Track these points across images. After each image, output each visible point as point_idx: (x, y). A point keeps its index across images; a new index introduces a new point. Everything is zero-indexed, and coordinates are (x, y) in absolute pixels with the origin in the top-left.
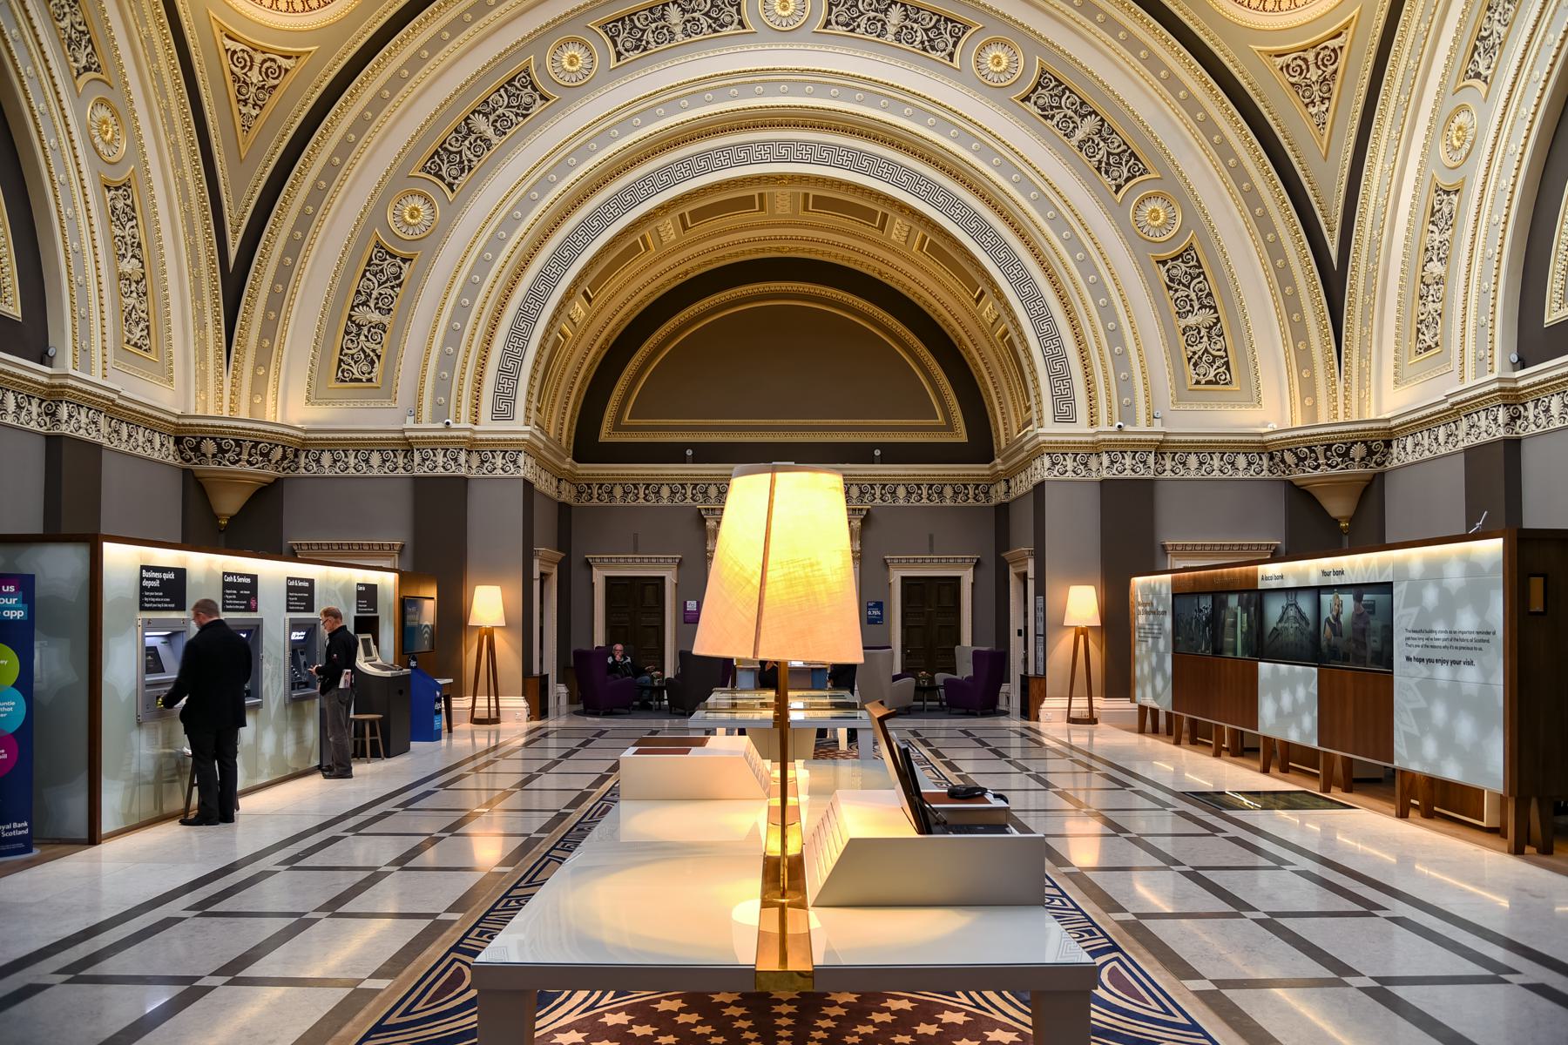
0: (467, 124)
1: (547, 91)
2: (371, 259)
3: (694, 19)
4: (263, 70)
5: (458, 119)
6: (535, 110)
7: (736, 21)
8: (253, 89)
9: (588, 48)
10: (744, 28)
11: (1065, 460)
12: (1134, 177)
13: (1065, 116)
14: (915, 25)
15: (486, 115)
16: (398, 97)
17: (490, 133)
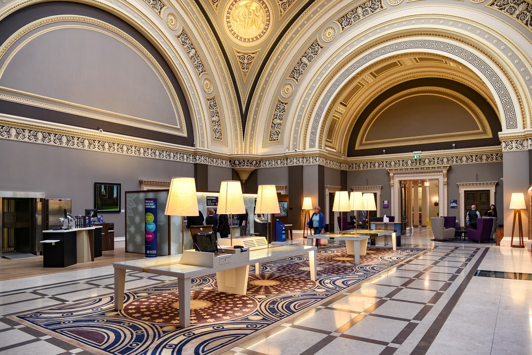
0: (301, 61)
2: (277, 105)
4: (248, 59)
5: (298, 60)
7: (380, 6)
8: (245, 65)
10: (382, 8)
11: (512, 143)
15: (306, 57)
16: (282, 57)
17: (307, 62)
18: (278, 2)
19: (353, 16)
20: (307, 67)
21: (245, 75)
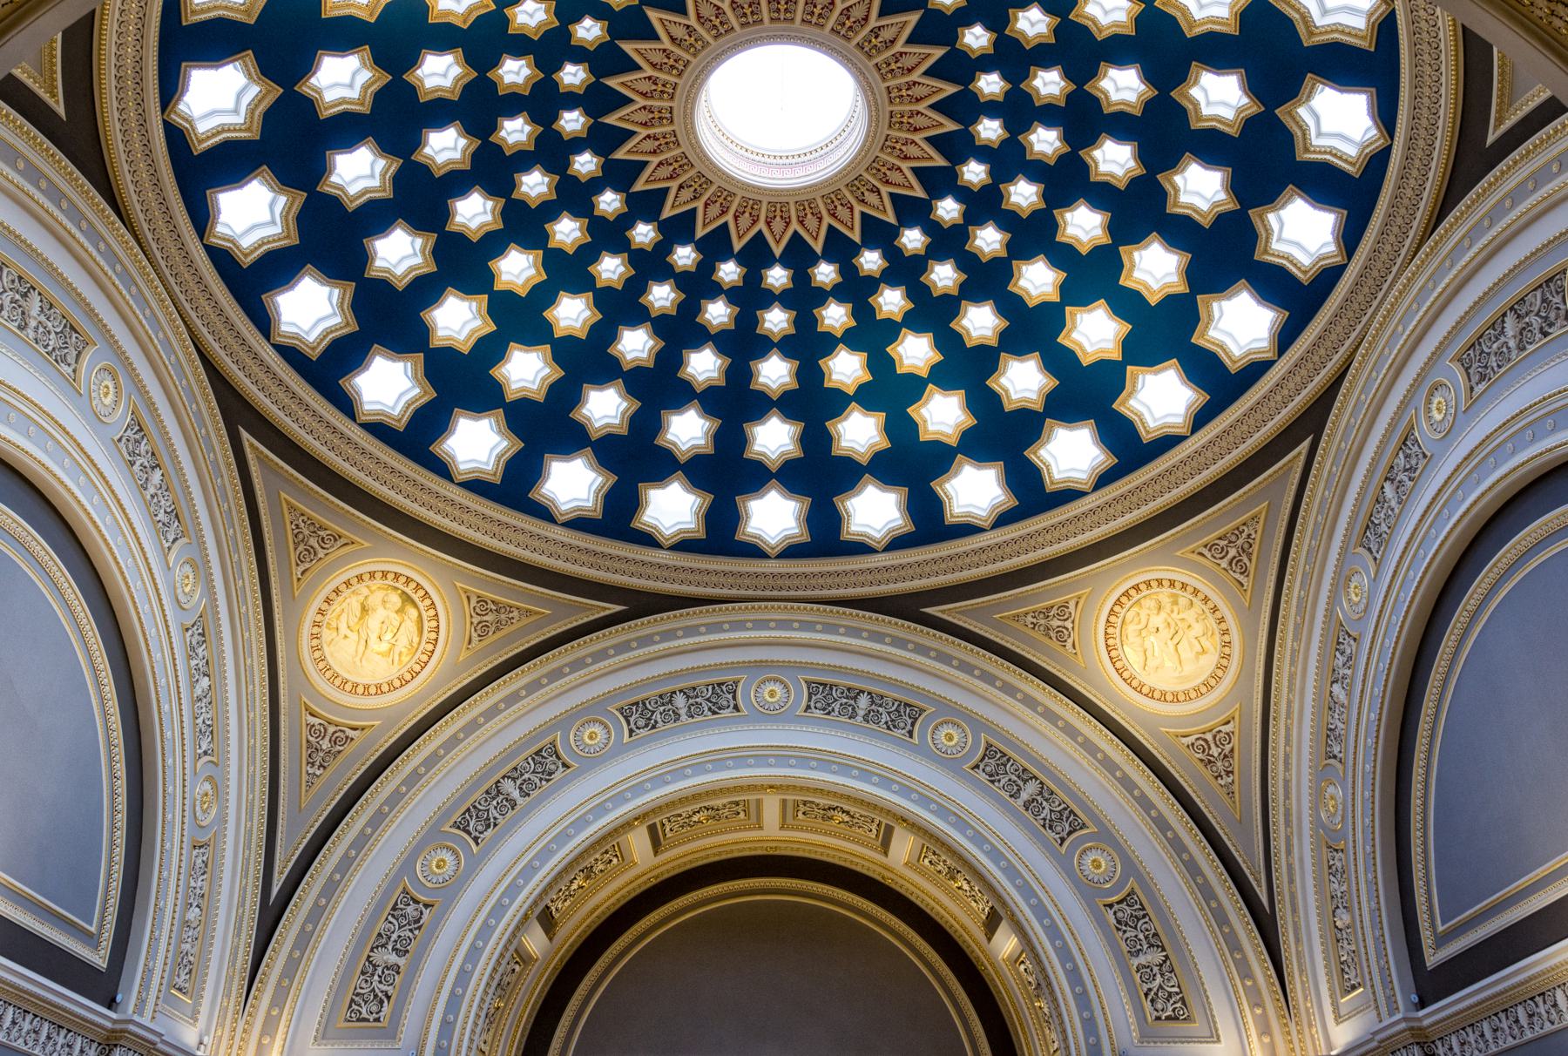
0: (497, 787)
1: (569, 761)
2: (396, 903)
3: (697, 703)
6: (557, 776)
7: (732, 706)
9: (606, 727)
10: (738, 711)
12: (1075, 830)
13: (1010, 780)
14: (880, 709)
15: (514, 779)
17: (516, 794)
18: (471, 616)
19: (662, 708)
20: (513, 809)
21: (310, 784)
